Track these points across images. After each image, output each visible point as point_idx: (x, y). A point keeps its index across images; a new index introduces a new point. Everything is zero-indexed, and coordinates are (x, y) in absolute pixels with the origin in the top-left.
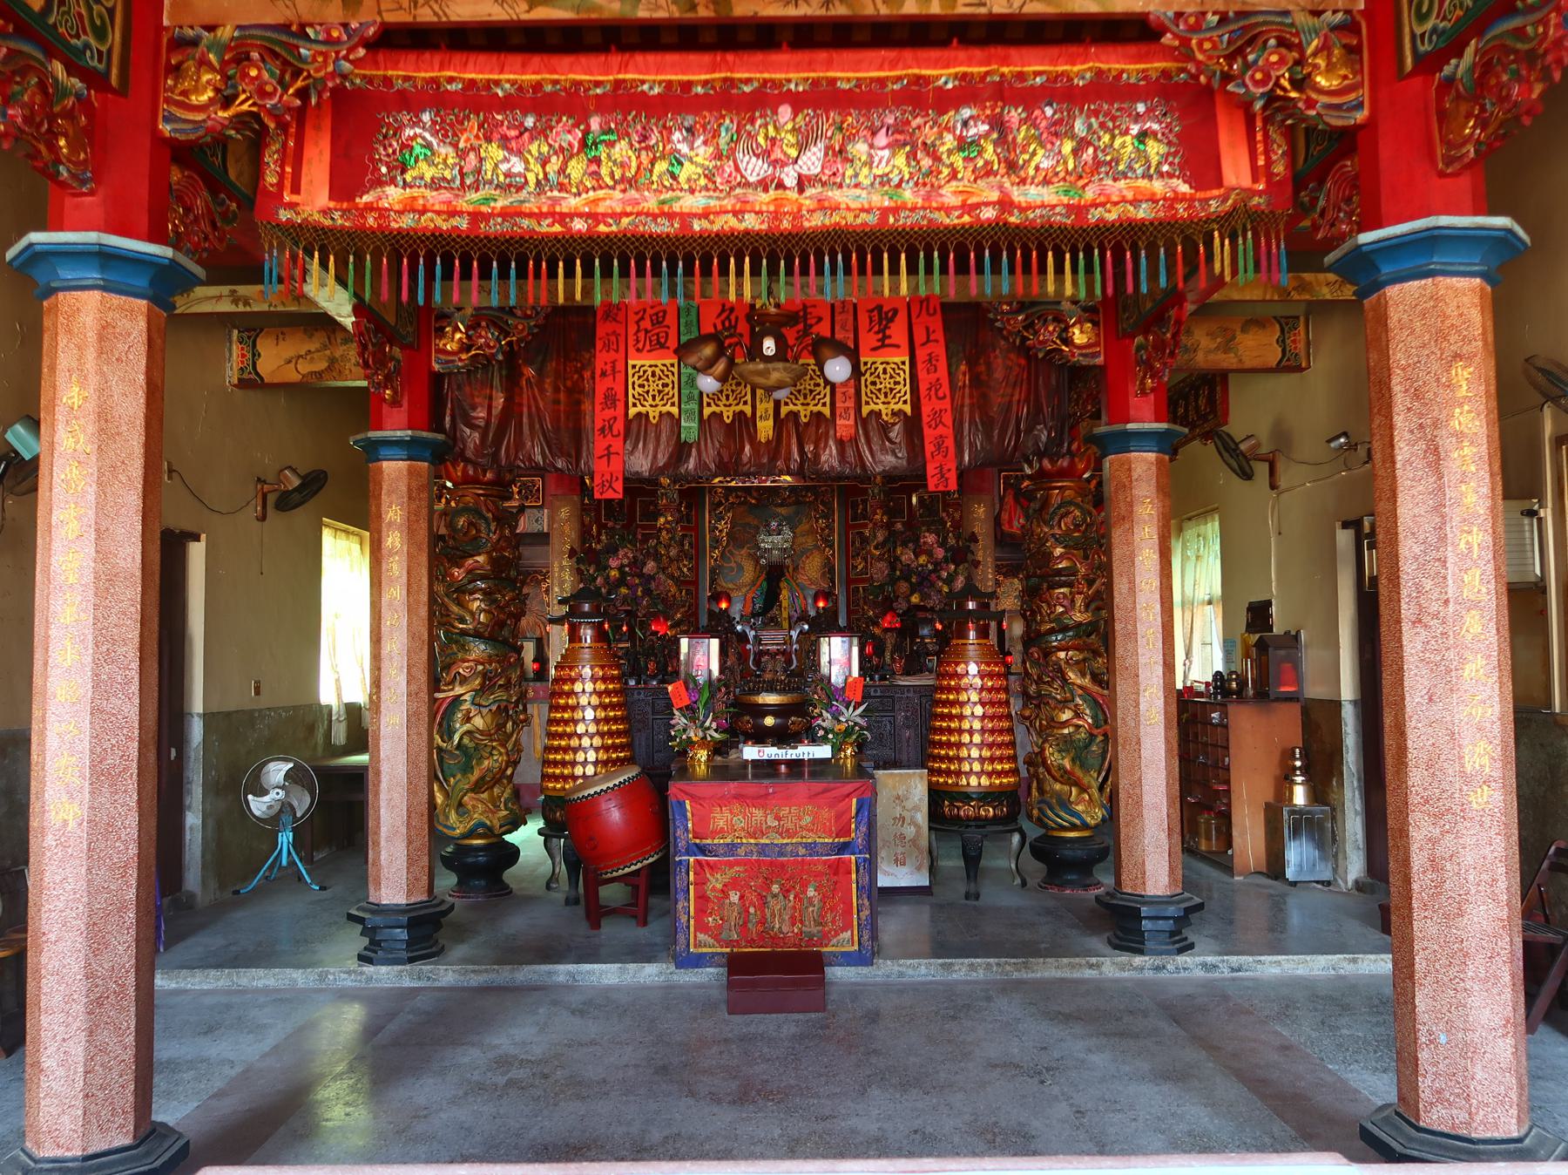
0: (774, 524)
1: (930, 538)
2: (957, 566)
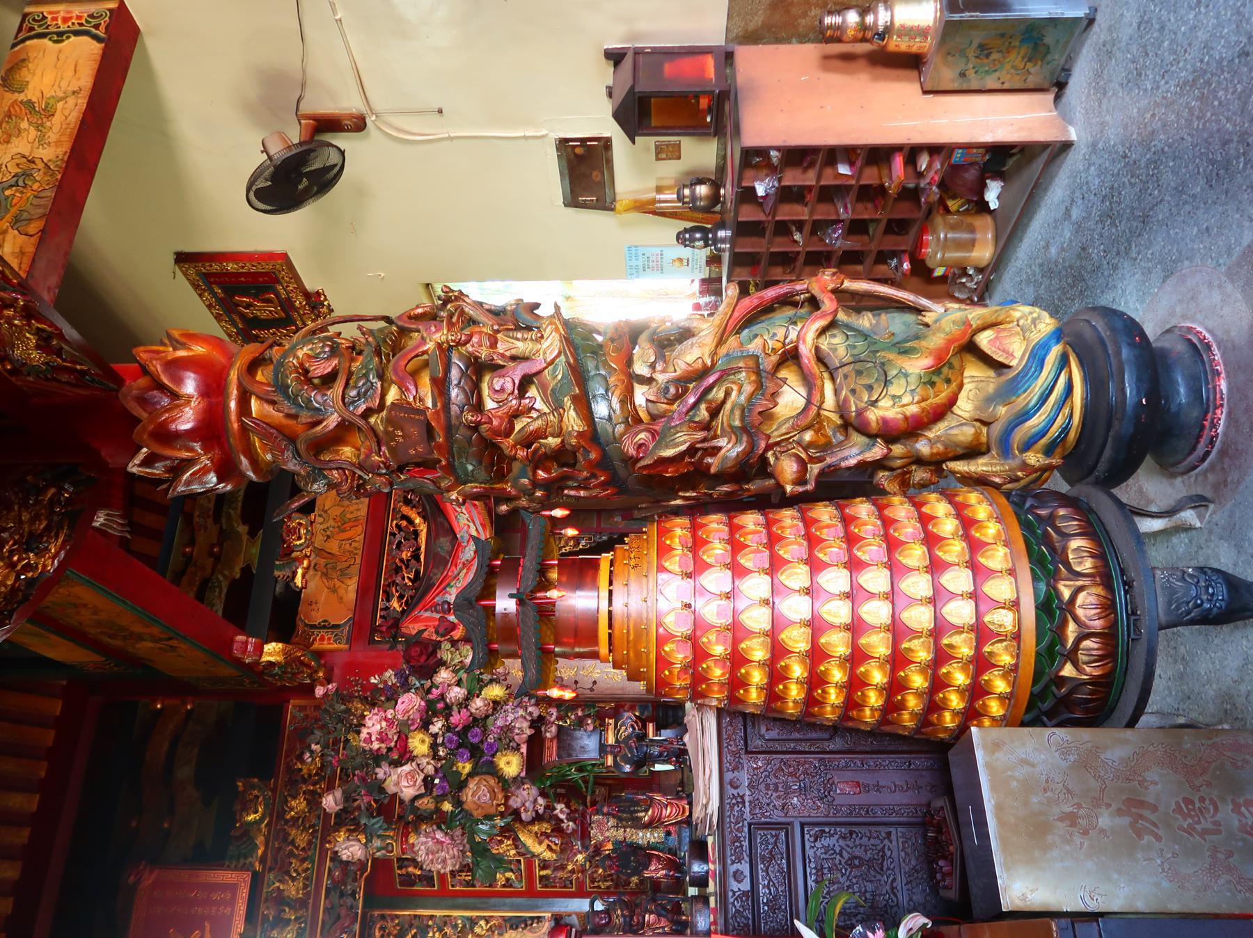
1: (374, 724)
2: (442, 663)
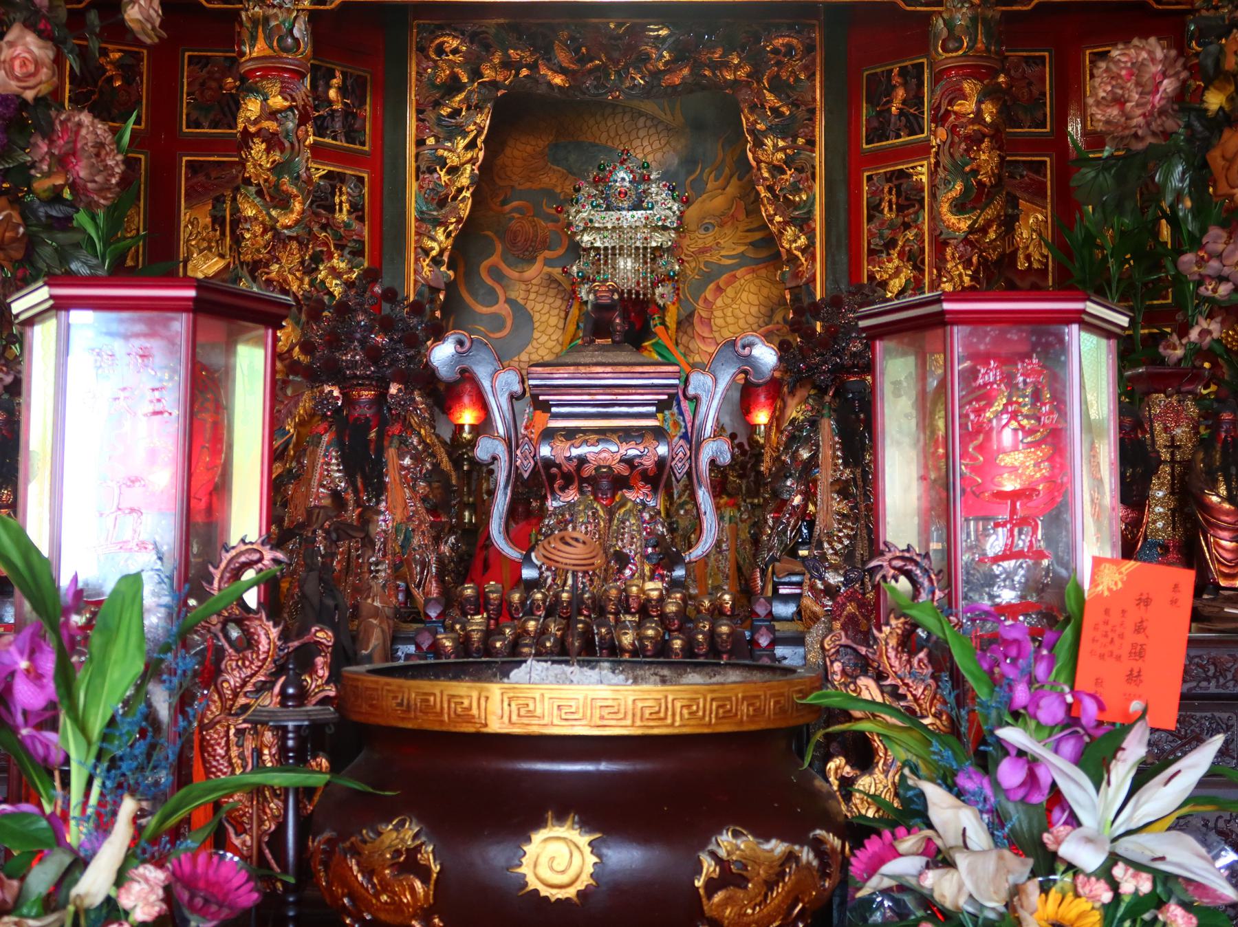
0: (622, 177)
